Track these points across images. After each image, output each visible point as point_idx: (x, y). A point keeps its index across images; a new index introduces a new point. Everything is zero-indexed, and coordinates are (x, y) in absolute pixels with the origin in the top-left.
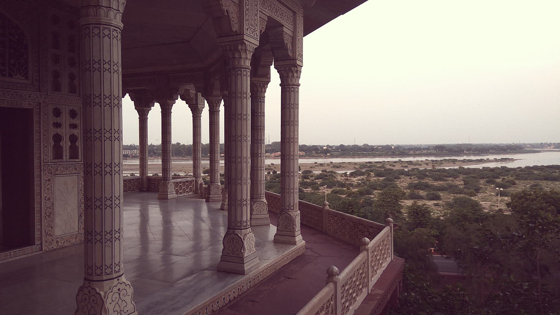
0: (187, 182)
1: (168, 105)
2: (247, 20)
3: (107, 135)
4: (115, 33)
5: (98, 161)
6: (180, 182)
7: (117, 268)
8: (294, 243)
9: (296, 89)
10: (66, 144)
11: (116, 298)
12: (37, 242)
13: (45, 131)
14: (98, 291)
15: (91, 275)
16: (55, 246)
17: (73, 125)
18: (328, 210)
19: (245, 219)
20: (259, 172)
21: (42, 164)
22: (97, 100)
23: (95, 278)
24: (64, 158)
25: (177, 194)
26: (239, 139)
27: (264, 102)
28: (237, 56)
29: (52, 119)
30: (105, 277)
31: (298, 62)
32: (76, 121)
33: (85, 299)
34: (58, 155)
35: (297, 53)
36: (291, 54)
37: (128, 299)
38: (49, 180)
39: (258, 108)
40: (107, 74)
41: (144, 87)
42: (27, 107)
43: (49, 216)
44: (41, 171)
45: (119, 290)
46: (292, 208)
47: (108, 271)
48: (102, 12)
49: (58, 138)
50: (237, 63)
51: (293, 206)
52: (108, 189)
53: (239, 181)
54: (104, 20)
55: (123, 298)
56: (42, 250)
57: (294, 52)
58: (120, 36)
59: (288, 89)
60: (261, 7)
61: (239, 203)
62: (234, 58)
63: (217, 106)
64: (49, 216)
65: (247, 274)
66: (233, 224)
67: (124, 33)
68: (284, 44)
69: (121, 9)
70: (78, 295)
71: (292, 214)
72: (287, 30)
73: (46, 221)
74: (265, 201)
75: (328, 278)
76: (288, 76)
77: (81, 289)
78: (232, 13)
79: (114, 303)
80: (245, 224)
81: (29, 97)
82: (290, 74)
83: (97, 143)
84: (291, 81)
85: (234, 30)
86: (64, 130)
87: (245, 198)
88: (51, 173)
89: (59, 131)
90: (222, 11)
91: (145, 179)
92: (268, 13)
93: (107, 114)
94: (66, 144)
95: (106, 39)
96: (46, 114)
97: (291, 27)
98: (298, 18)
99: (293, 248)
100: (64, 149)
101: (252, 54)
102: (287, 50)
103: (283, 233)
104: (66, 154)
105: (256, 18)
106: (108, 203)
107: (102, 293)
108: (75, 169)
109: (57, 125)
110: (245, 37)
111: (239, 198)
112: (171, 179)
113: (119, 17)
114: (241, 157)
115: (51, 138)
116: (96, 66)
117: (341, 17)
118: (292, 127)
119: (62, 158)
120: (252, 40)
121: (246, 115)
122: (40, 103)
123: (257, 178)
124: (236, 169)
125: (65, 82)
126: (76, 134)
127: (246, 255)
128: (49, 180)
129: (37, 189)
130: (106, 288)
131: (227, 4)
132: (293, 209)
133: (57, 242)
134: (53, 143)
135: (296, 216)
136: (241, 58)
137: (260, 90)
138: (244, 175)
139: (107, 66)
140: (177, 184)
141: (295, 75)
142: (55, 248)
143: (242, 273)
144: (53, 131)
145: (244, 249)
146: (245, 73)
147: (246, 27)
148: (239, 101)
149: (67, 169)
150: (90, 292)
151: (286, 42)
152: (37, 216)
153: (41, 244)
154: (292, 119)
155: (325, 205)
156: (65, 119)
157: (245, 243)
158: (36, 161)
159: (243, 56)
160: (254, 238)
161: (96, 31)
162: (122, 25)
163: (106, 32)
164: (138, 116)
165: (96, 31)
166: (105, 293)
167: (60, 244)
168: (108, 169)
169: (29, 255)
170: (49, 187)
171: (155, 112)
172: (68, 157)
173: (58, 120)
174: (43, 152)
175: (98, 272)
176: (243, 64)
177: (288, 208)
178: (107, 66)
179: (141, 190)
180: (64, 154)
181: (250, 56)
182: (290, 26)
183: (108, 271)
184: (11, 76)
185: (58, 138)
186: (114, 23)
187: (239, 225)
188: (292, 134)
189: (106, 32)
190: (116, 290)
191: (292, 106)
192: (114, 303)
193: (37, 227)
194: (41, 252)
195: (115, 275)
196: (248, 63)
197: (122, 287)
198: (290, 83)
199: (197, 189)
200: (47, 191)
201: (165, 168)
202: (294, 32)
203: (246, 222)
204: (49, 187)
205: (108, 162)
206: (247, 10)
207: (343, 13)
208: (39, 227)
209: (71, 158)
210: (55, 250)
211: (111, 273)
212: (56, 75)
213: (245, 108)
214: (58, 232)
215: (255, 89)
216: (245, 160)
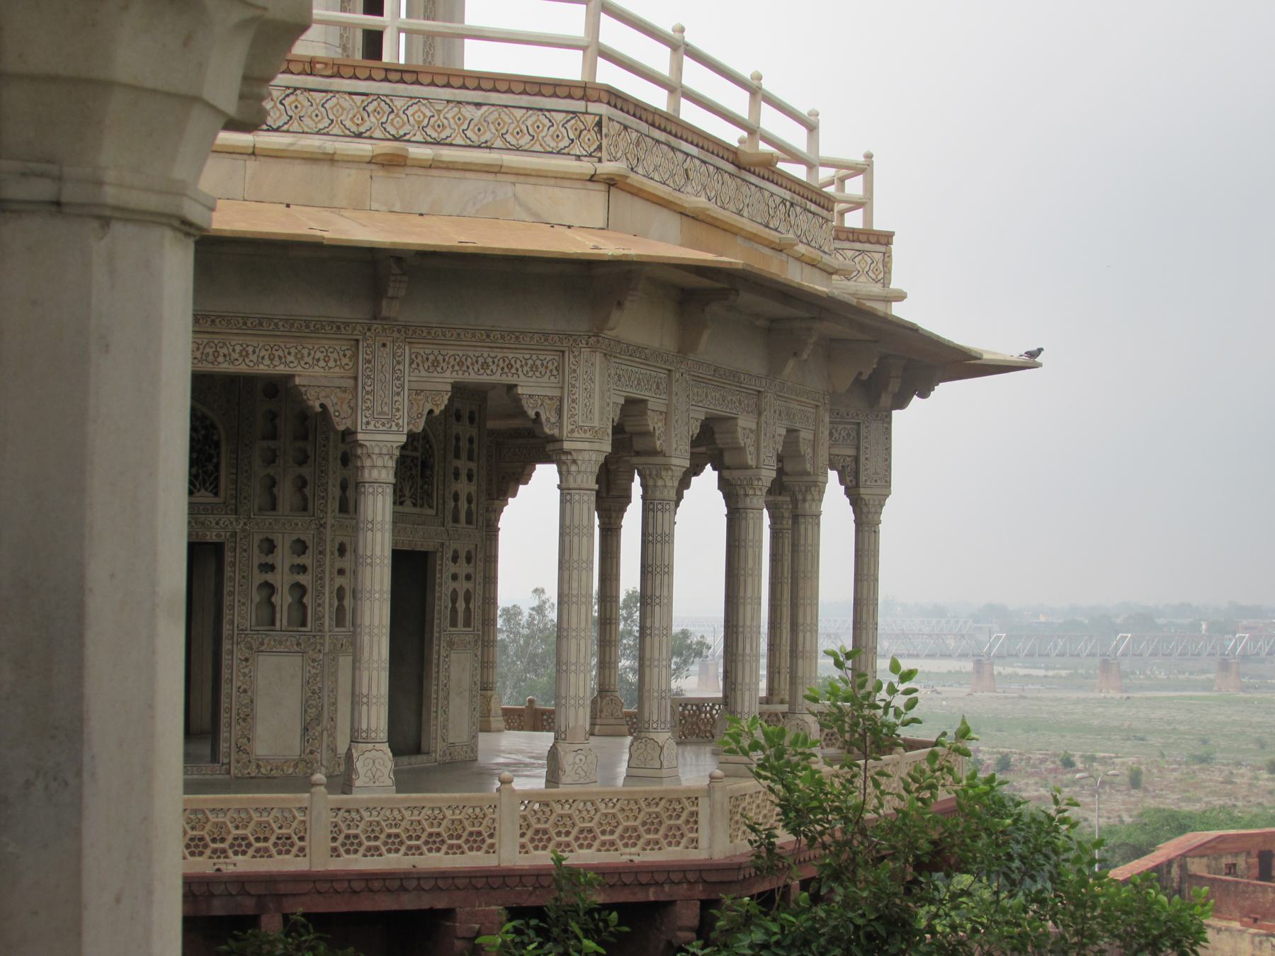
10: (283, 599)
17: (298, 565)
24: (278, 623)
29: (258, 558)
32: (306, 560)
42: (215, 539)
49: (269, 588)
63: (804, 500)
64: (244, 720)
80: (364, 735)
81: (217, 523)
84: (575, 481)
86: (279, 577)
88: (251, 648)
89: (269, 577)
94: (283, 599)
100: (278, 608)
104: (282, 618)
108: (298, 644)
109: (271, 568)
110: (360, 437)
125: (286, 492)
126: (304, 582)
128: (247, 660)
131: (322, 394)
133: (258, 766)
144: (259, 578)
145: (357, 773)
149: (280, 643)
153: (229, 763)
156: (283, 558)
159: (368, 463)
167: (263, 770)
170: (247, 671)
172: (285, 622)
173: (269, 559)
180: (278, 616)
209: (289, 623)
213: (369, 547)
214: (261, 748)
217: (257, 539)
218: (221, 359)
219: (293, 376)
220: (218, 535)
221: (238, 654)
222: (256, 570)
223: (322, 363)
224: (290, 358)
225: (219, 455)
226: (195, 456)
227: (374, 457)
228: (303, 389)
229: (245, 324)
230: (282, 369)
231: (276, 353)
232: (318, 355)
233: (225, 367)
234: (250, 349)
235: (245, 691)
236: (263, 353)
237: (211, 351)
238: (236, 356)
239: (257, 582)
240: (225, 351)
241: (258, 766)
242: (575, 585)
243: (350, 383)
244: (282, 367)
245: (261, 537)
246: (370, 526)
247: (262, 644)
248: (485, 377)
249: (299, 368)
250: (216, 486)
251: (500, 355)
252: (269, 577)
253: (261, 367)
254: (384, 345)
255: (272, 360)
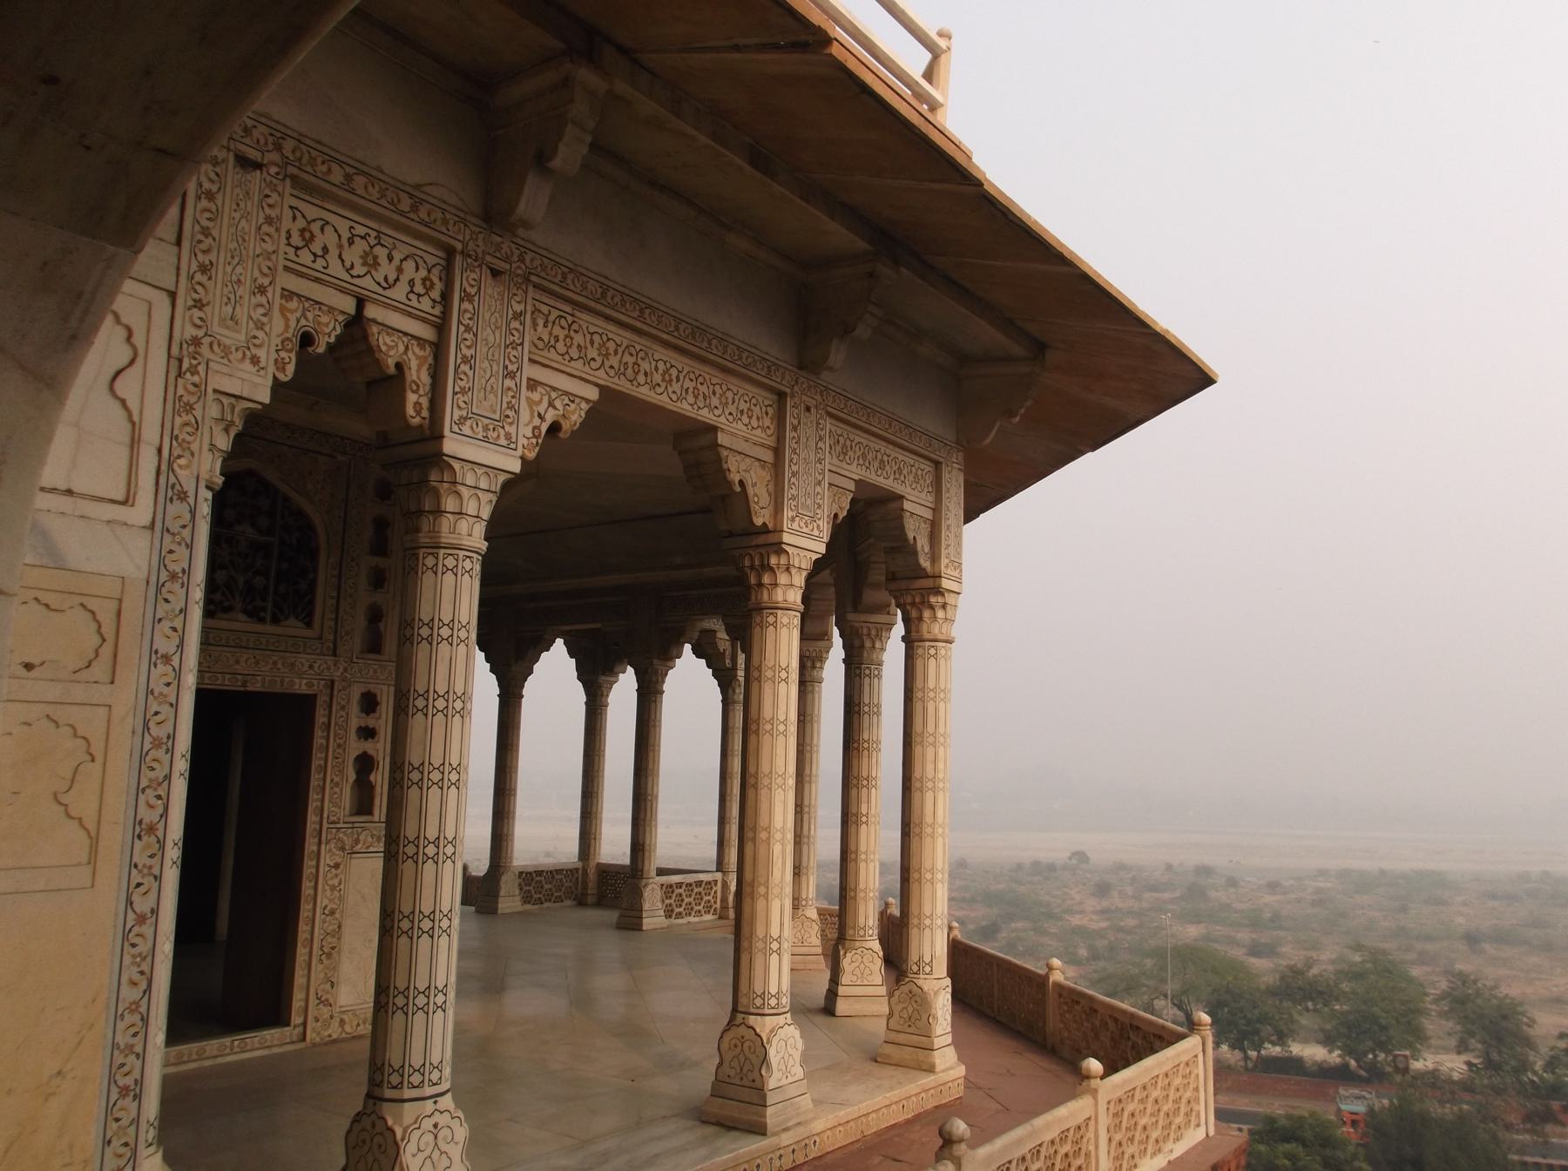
0: (699, 884)
1: (656, 673)
2: (793, 498)
3: (435, 776)
4: (468, 564)
5: (411, 834)
6: (679, 885)
7: (435, 1076)
8: (931, 1069)
9: (943, 652)
11: (427, 1144)
12: (296, 1019)
13: (339, 746)
14: (390, 1122)
15: (380, 1085)
16: (334, 1031)
18: (1057, 985)
19: (773, 990)
20: (862, 866)
21: (325, 825)
22: (420, 703)
23: (388, 1093)
25: (669, 913)
26: (766, 782)
27: (879, 677)
28: (766, 579)
29: (356, 720)
30: (408, 1093)
31: (946, 584)
33: (364, 1142)
34: (363, 805)
35: (944, 561)
36: (925, 563)
37: (456, 1152)
38: (337, 866)
39: (861, 692)
40: (444, 646)
41: (598, 625)
43: (329, 955)
44: (320, 843)
45: (435, 1126)
46: (928, 969)
47: (416, 1078)
48: (446, 522)
49: (365, 764)
50: (765, 597)
51: (930, 964)
52: (427, 893)
53: (762, 890)
54: (446, 537)
55: (443, 1146)
56: (304, 1039)
57: (935, 557)
58: (478, 567)
59: (920, 651)
60: (835, 461)
61: (760, 945)
62: (760, 585)
64: (329, 955)
65: (775, 1134)
66: (743, 1000)
67: (488, 562)
68: (906, 540)
69: (486, 513)
70: (349, 1132)
71: (927, 984)
72: (916, 504)
73: (321, 967)
74: (876, 946)
75: (942, 1147)
76: (920, 619)
77: (357, 1118)
78: (754, 485)
79: (421, 1156)
80: (773, 1002)
81: (311, 667)
82: (927, 614)
83: (413, 793)
85: (758, 521)
86: (380, 746)
87: (775, 932)
88: (343, 849)
89: (369, 746)
90: (729, 484)
91: (592, 872)
92: (856, 471)
93: (438, 732)
94: (380, 779)
95: (449, 577)
96: (343, 708)
97: (928, 499)
98: (945, 476)
99: (927, 1080)
100: (378, 789)
101: (804, 574)
102: (915, 553)
103: (901, 1038)
105: (818, 489)
106: (426, 925)
107: (399, 1132)
109: (368, 733)
110: (786, 538)
111: (760, 932)
112: (653, 873)
113: (480, 529)
114: (768, 829)
115: (351, 762)
116: (425, 632)
117: (1089, 458)
118: (930, 752)
119: (370, 813)
120: (805, 540)
121: (785, 722)
122: (333, 682)
123: (857, 884)
124: (754, 859)
127: (772, 1083)
128: (337, 866)
129: (307, 888)
130: (408, 1119)
131: (743, 466)
132: (931, 973)
133: (342, 1022)
134: (352, 776)
135: (936, 993)
136: (776, 585)
137: (868, 644)
138: (777, 873)
139: (445, 632)
140: (669, 890)
141: (940, 614)
142: (335, 1036)
143: (759, 1130)
144: (356, 747)
145: (769, 1067)
146: (785, 620)
147: (788, 513)
148: (767, 689)
150: (374, 1125)
151: (910, 536)
152: (301, 953)
153: (305, 1024)
154: (930, 728)
155: (1050, 968)
157: (772, 1052)
158: (312, 818)
159: (783, 579)
160: (800, 1044)
161: (430, 561)
162: (484, 545)
163: (450, 562)
164: (584, 699)
165: (430, 561)
166: (405, 1131)
167: (348, 1028)
168: (431, 850)
169: (275, 1050)
170: (336, 882)
171: (624, 689)
173: (371, 722)
174: (330, 795)
175: (395, 1079)
176: (780, 599)
177: (915, 968)
178: (445, 632)
179: (581, 903)
181: (799, 580)
182: (923, 495)
183: (416, 1078)
184: (275, 620)
185: (365, 764)
186: (466, 542)
187: (758, 1002)
188: (930, 767)
189: (450, 562)
190: (427, 1124)
191: (932, 694)
192: (421, 1156)
193: (299, 979)
194: (302, 1045)
195: (429, 1091)
196: (795, 597)
197: (442, 1119)
198: (927, 636)
199: (725, 907)
200: (328, 893)
201: (639, 846)
202: (936, 510)
203: (778, 996)
204: (336, 882)
205: (432, 833)
206: (794, 474)
207: (1095, 446)
208: (303, 981)
210: (335, 1041)
211: (420, 1085)
212: (375, 616)
213: (782, 707)
215: (857, 643)
216: (778, 836)
217: (356, 693)
218: (641, 378)
219: (713, 429)
220: (310, 685)
221: (327, 859)
222: (353, 736)
223: (745, 419)
224: (715, 401)
225: (315, 570)
226: (221, 576)
227: (793, 571)
228: (725, 453)
229: (677, 329)
230: (705, 415)
231: (703, 389)
232: (743, 406)
233: (644, 393)
234: (674, 372)
235: (332, 913)
236: (687, 384)
237: (631, 360)
238: (657, 378)
239: (353, 754)
240: (645, 366)
241: (342, 1022)
242: (941, 766)
243: (768, 456)
244: (705, 412)
245: (363, 690)
246: (783, 675)
247: (357, 841)
248: (881, 479)
249: (722, 419)
250: (310, 614)
251: (894, 455)
252: (369, 746)
253: (685, 406)
254: (808, 409)
255: (696, 397)
